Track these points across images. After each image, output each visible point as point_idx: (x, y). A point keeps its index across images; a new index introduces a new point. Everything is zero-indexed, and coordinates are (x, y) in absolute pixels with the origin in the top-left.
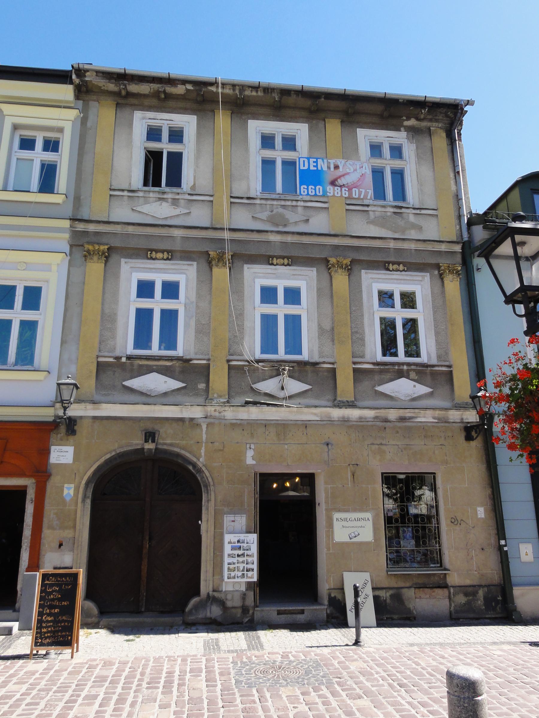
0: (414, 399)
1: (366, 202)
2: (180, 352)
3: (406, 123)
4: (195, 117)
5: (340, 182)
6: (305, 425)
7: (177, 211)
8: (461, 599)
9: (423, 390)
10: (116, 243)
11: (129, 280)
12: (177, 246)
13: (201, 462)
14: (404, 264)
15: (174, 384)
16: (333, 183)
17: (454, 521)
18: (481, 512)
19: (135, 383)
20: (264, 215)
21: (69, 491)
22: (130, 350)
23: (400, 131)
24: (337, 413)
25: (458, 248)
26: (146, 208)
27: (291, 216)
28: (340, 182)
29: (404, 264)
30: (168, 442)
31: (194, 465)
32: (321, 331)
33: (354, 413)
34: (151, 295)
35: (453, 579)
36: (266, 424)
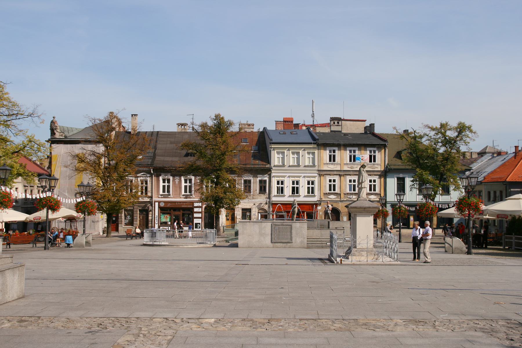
0: (374, 199)
1: (368, 163)
3: (377, 146)
4: (337, 148)
5: (363, 159)
7: (335, 167)
9: (376, 197)
11: (327, 180)
13: (340, 209)
14: (374, 175)
16: (362, 160)
19: (329, 197)
21: (321, 213)
22: (328, 192)
23: (375, 148)
25: (384, 172)
28: (363, 159)
29: (374, 175)
30: (335, 206)
31: (339, 209)
34: (331, 182)
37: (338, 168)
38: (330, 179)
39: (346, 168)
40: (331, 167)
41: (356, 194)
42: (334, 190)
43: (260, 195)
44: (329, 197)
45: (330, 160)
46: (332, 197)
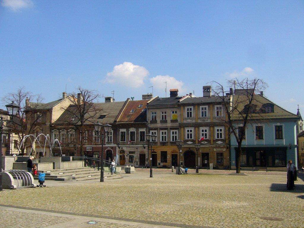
2: (192, 139)
6: (207, 147)
8: (225, 167)
9: (222, 142)
10: (184, 125)
12: (191, 125)
15: (192, 143)
17: (225, 158)
18: (228, 157)
19: (187, 143)
20: (202, 120)
21: (182, 155)
22: (187, 139)
24: (211, 146)
26: (188, 120)
27: (205, 120)
32: (209, 135)
33: (213, 146)
35: (224, 165)
36: (202, 147)
37: (194, 121)
38: (188, 129)
39: (199, 121)
40: (189, 121)
41: (206, 140)
42: (191, 138)
43: (140, 142)
44: (187, 143)
45: (188, 116)
46: (190, 143)
